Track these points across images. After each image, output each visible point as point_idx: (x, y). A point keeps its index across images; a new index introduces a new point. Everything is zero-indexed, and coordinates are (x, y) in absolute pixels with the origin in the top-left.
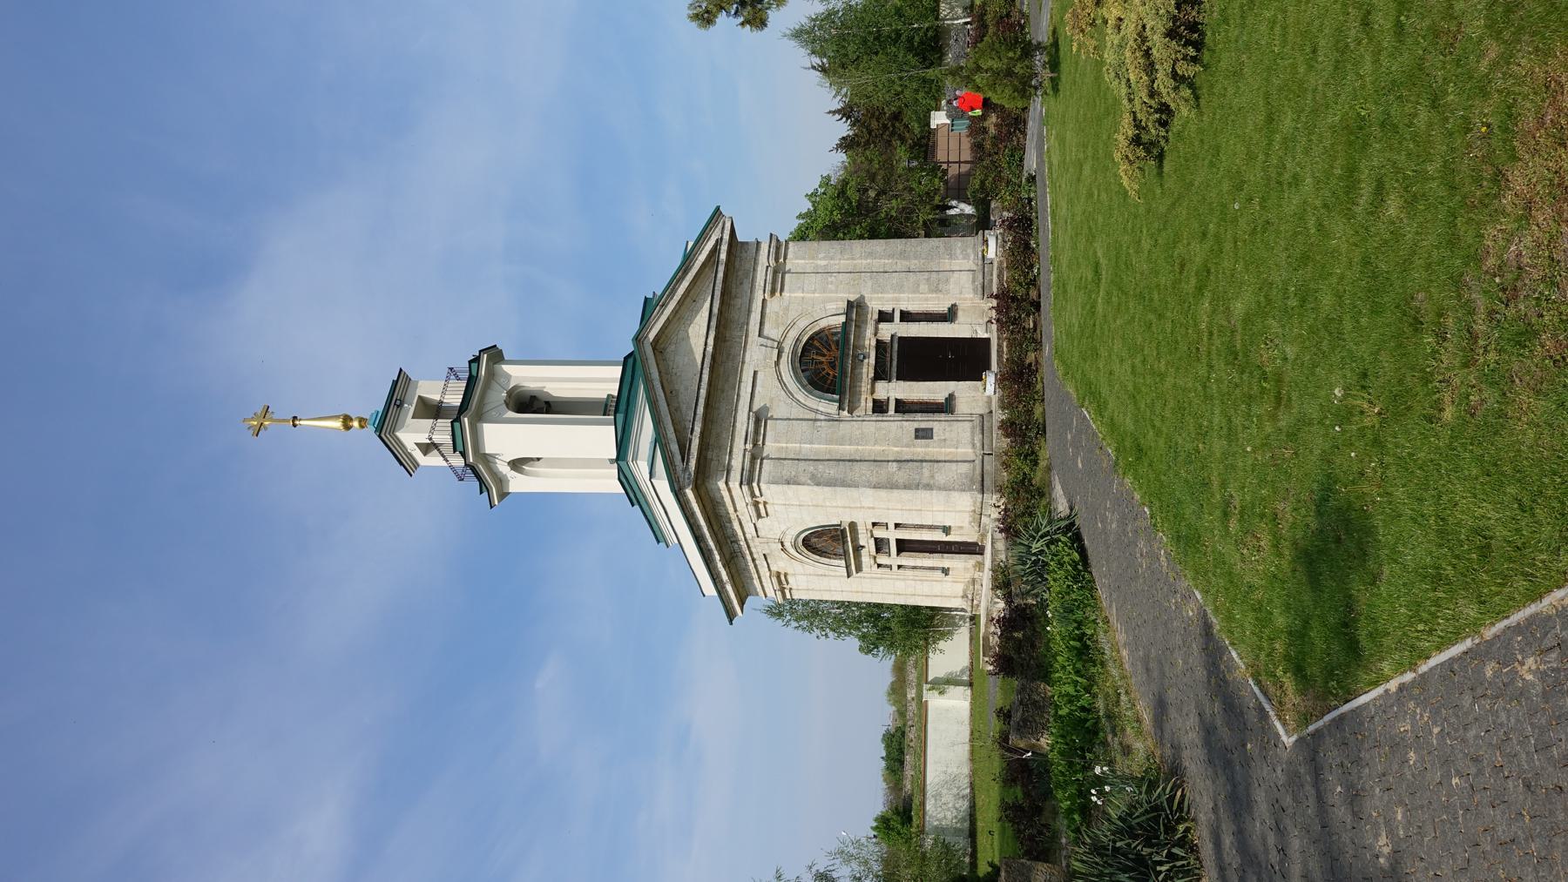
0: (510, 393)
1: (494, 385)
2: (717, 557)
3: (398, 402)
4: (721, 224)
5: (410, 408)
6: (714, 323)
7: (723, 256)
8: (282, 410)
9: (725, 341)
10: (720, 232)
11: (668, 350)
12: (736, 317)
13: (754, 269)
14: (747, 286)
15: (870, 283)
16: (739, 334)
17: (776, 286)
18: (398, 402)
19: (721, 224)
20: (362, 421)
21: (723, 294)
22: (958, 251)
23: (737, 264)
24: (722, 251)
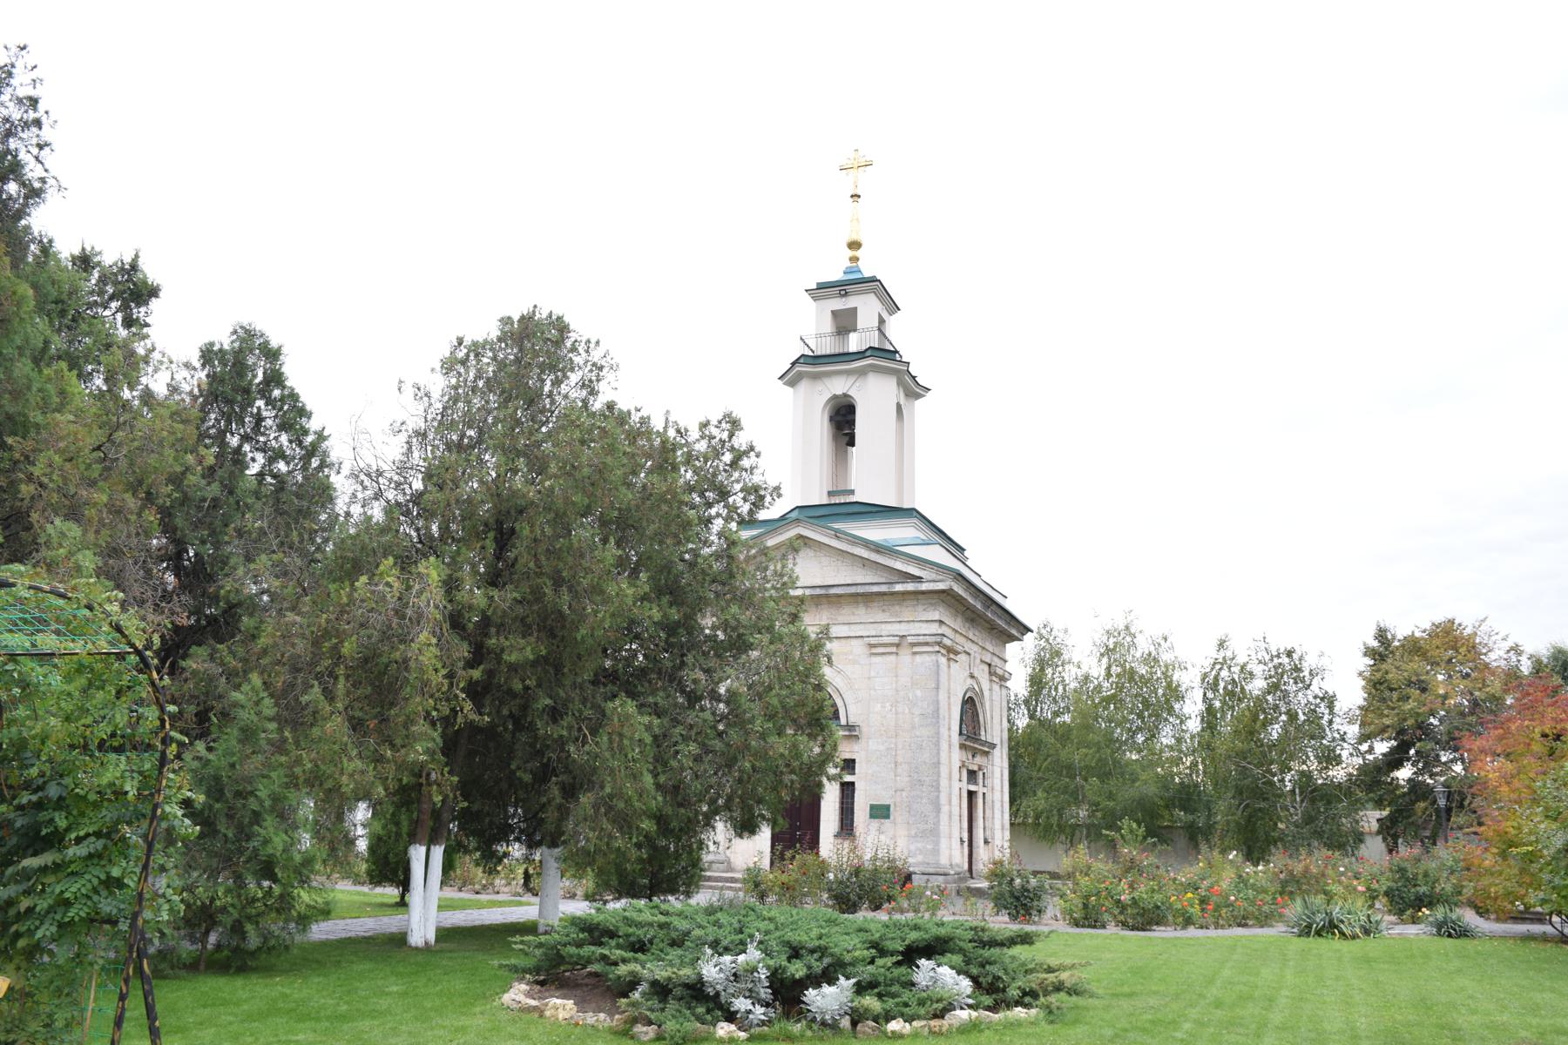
0: (845, 395)
1: (852, 379)
2: (971, 601)
3: (843, 292)
4: (941, 577)
5: (839, 304)
6: (818, 591)
7: (899, 588)
8: (865, 182)
9: (817, 605)
10: (930, 578)
11: (808, 550)
12: (844, 612)
13: (900, 622)
14: (881, 617)
15: (882, 748)
16: (824, 617)
17: (875, 647)
18: (843, 292)
19: (941, 577)
20: (854, 259)
21: (857, 595)
22: (919, 845)
23: (909, 602)
24: (905, 585)
